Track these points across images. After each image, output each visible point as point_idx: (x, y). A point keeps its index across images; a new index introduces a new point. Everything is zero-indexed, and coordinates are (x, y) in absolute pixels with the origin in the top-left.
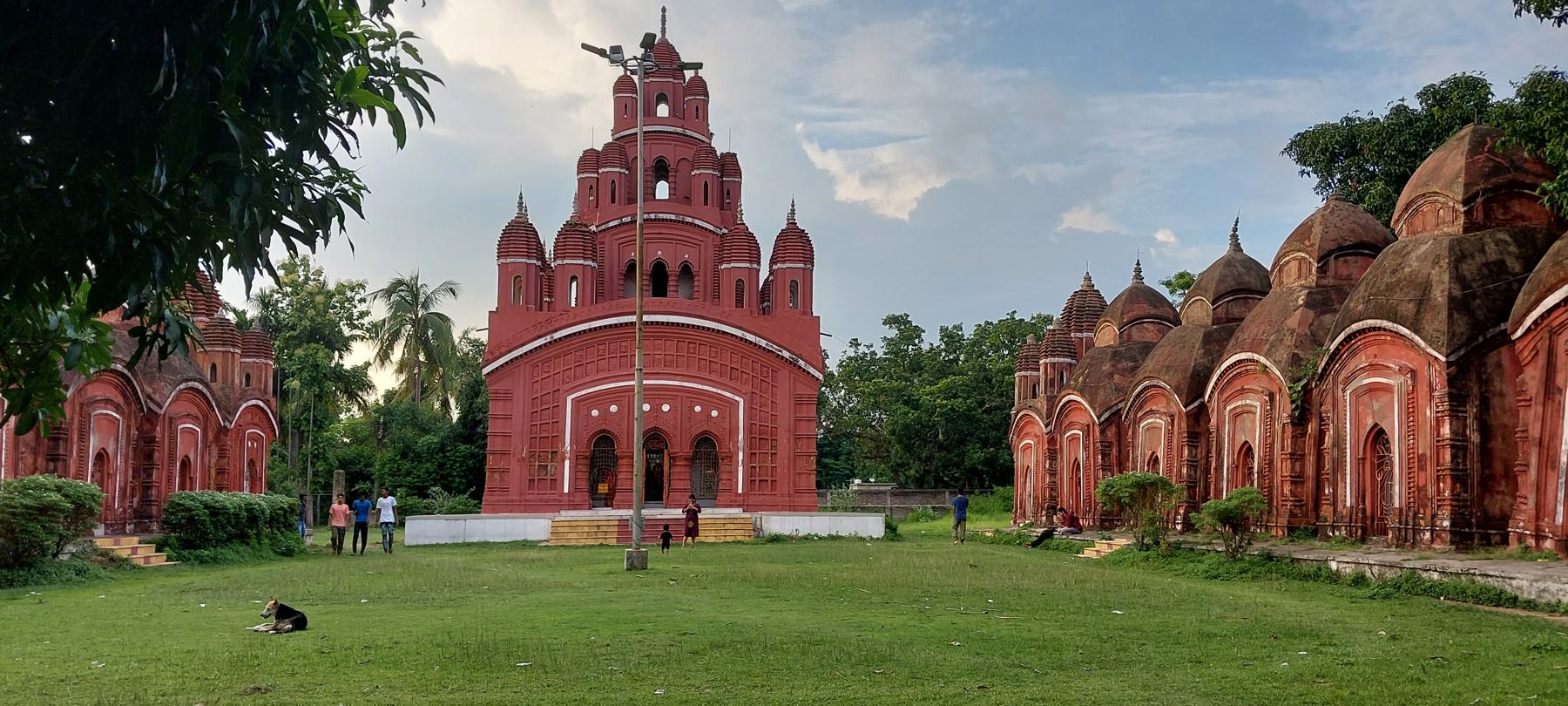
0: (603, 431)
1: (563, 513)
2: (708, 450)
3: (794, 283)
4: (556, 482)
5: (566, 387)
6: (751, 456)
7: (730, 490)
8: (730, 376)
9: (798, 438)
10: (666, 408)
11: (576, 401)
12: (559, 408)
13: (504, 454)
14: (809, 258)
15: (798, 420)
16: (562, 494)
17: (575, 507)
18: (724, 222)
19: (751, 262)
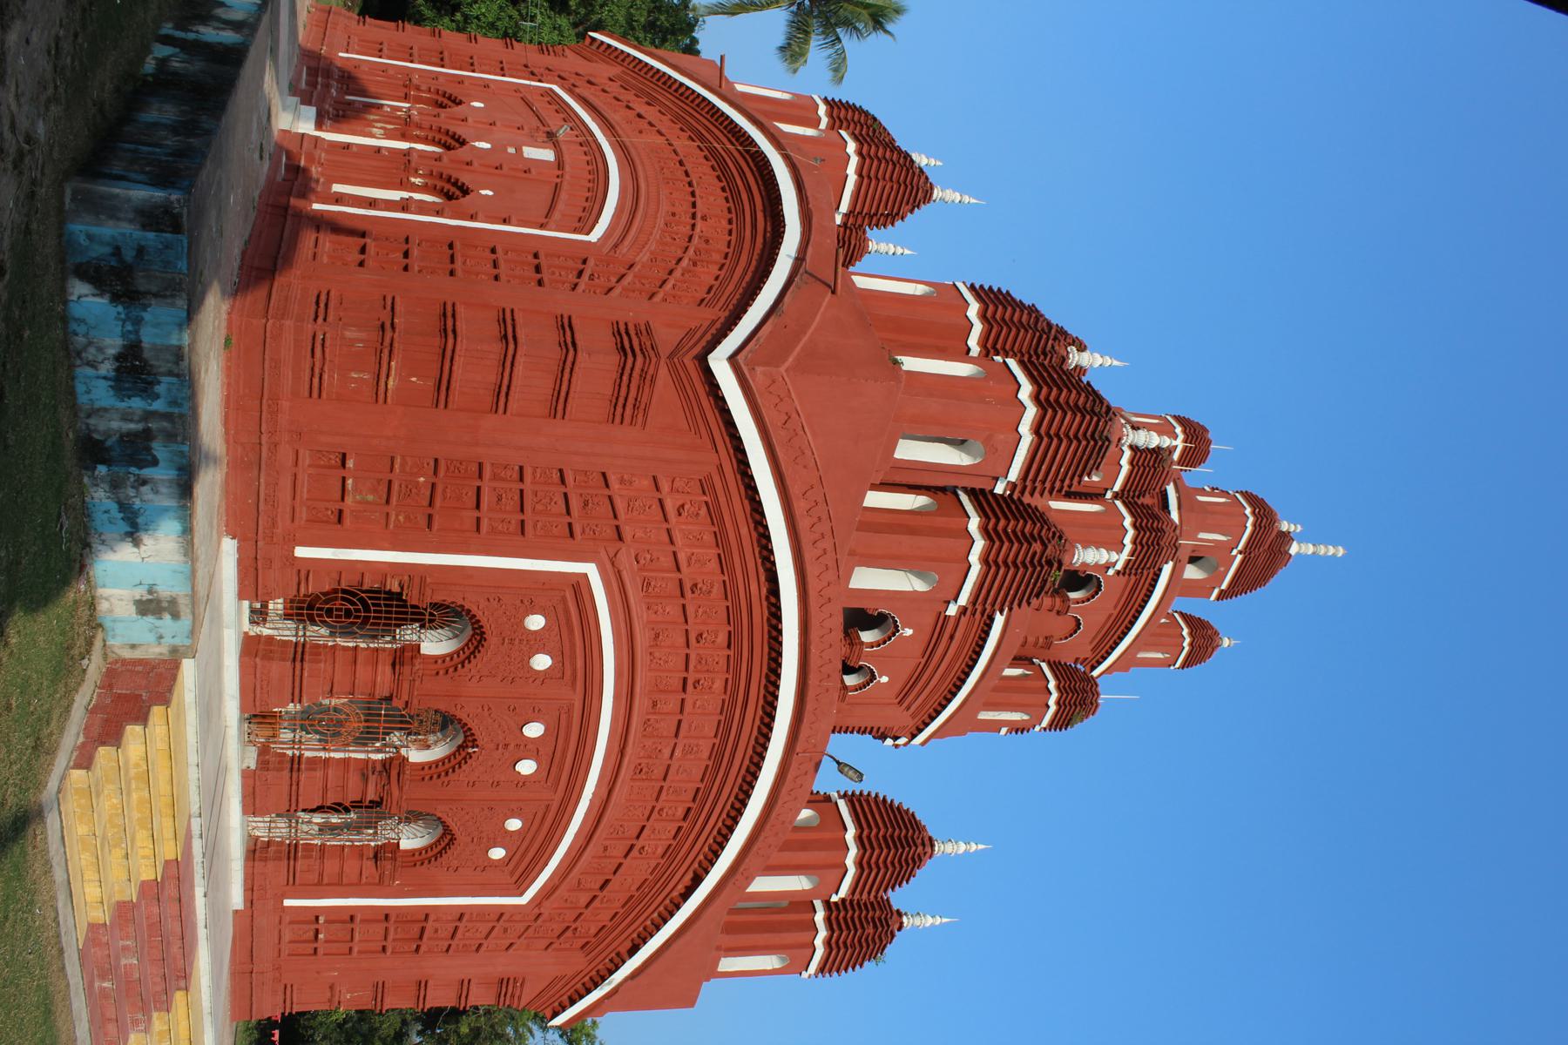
1: (229, 547)
4: (335, 527)
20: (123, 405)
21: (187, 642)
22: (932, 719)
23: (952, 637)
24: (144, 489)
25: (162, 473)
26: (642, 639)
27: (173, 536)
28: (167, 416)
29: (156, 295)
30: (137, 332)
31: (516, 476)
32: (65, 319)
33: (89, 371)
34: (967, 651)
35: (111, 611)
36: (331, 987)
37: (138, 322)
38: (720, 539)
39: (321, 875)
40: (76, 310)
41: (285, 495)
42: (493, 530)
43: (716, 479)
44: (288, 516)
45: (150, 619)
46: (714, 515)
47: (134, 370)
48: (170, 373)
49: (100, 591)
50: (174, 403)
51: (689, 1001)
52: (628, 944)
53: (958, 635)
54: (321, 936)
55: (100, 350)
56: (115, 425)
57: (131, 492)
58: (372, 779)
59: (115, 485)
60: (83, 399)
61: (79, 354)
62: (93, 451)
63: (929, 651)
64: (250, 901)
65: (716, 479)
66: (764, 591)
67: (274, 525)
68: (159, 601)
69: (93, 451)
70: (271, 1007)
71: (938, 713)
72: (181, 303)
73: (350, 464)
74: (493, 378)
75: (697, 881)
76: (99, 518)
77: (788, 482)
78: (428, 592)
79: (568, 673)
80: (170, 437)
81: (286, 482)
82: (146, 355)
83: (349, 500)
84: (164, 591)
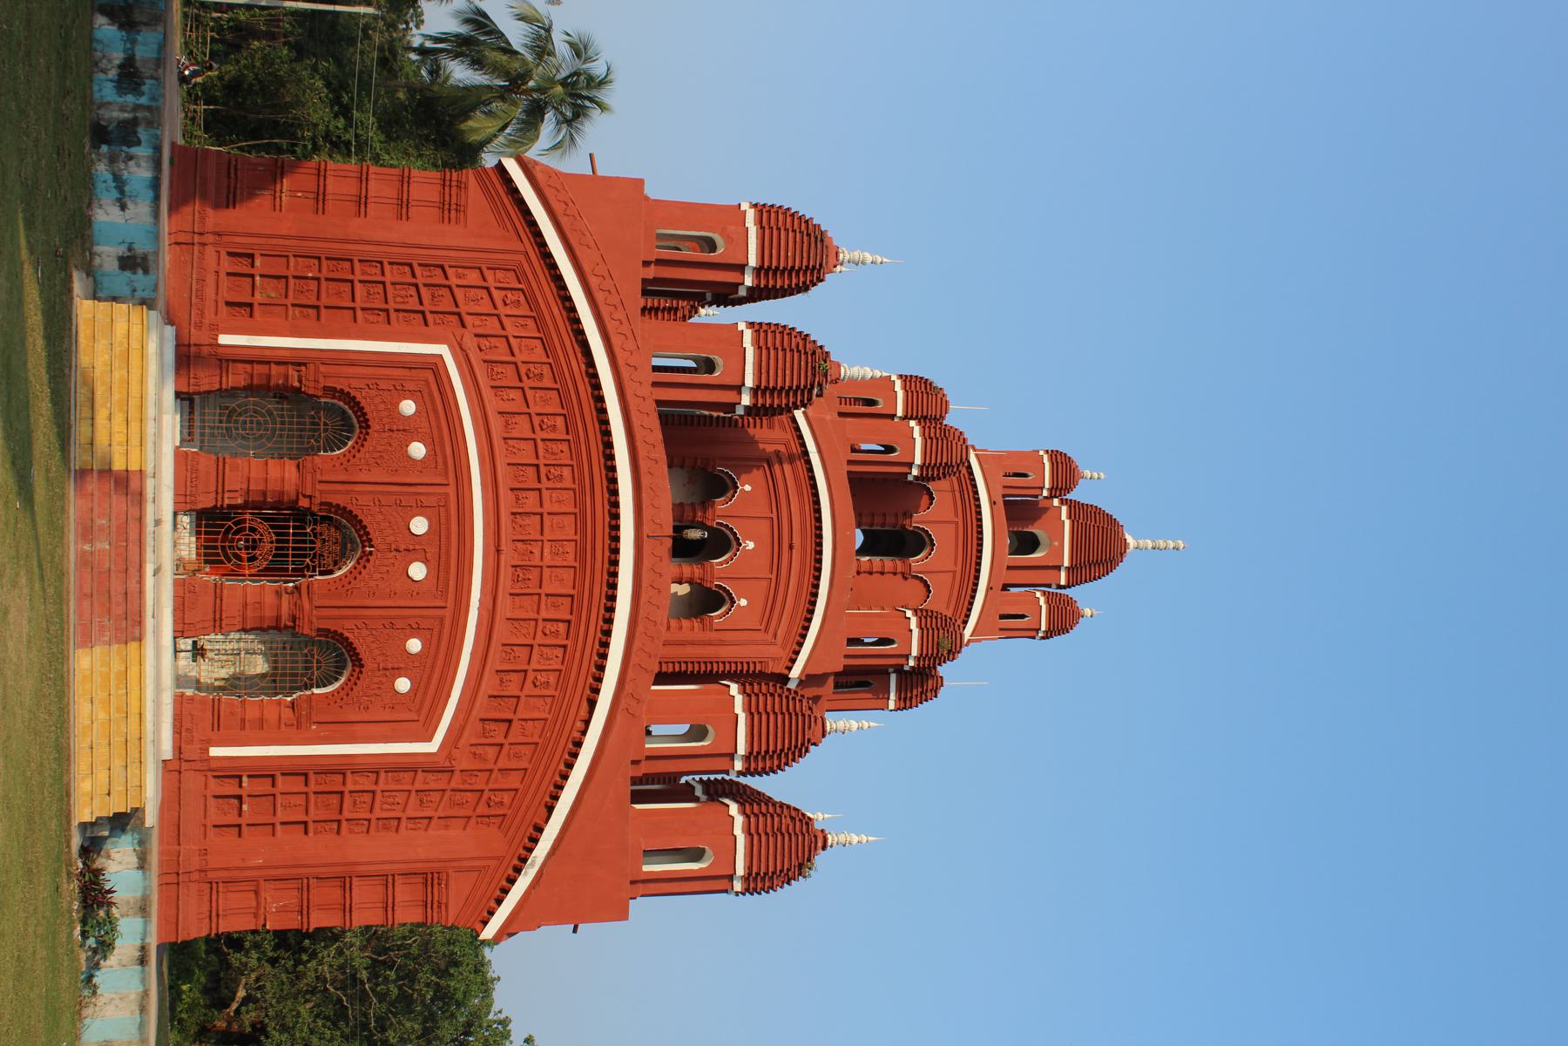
0: (365, 424)
2: (319, 659)
3: (697, 855)
5: (470, 342)
6: (300, 770)
7: (217, 723)
8: (491, 718)
9: (344, 882)
10: (418, 571)
11: (434, 366)
12: (421, 322)
13: (320, 197)
14: (759, 882)
15: (387, 880)
16: (217, 329)
17: (186, 358)
18: (808, 680)
19: (747, 758)
20: (120, 100)
21: (152, 295)
22: (801, 645)
23: (791, 547)
24: (131, 163)
25: (143, 152)
26: (496, 424)
27: (148, 202)
28: (149, 108)
29: (146, 24)
30: (132, 49)
31: (378, 271)
32: (91, 40)
33: (102, 76)
34: (810, 561)
35: (101, 266)
36: (256, 892)
37: (134, 42)
38: (538, 320)
39: (243, 720)
40: (98, 35)
41: (210, 291)
42: (367, 321)
43: (526, 266)
44: (213, 310)
45: (128, 274)
46: (531, 302)
47: (129, 76)
48: (152, 77)
49: (97, 249)
50: (153, 99)
51: (623, 915)
52: (544, 811)
53: (796, 541)
54: (245, 807)
55: (110, 61)
56: (115, 114)
57: (122, 166)
58: (285, 597)
59: (112, 160)
60: (97, 96)
61: (96, 64)
62: (100, 134)
63: (776, 564)
64: (178, 749)
65: (526, 266)
66: (583, 367)
67: (202, 314)
68: (133, 258)
69: (100, 134)
70: (195, 928)
71: (804, 636)
72: (160, 29)
73: (258, 263)
74: (354, 191)
75: (592, 704)
76: (100, 186)
77: (578, 253)
78: (322, 380)
79: (440, 461)
80: (150, 124)
81: (211, 279)
82: (138, 64)
83: (257, 295)
84: (140, 249)
